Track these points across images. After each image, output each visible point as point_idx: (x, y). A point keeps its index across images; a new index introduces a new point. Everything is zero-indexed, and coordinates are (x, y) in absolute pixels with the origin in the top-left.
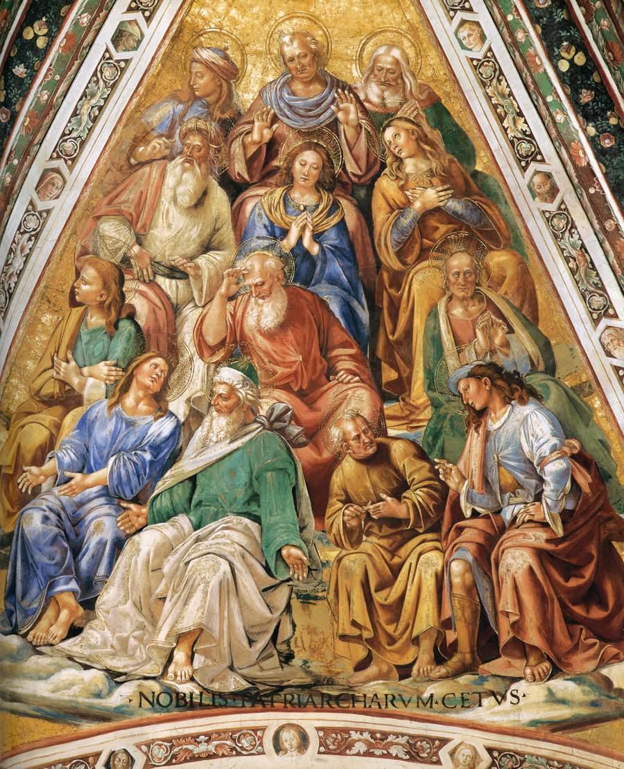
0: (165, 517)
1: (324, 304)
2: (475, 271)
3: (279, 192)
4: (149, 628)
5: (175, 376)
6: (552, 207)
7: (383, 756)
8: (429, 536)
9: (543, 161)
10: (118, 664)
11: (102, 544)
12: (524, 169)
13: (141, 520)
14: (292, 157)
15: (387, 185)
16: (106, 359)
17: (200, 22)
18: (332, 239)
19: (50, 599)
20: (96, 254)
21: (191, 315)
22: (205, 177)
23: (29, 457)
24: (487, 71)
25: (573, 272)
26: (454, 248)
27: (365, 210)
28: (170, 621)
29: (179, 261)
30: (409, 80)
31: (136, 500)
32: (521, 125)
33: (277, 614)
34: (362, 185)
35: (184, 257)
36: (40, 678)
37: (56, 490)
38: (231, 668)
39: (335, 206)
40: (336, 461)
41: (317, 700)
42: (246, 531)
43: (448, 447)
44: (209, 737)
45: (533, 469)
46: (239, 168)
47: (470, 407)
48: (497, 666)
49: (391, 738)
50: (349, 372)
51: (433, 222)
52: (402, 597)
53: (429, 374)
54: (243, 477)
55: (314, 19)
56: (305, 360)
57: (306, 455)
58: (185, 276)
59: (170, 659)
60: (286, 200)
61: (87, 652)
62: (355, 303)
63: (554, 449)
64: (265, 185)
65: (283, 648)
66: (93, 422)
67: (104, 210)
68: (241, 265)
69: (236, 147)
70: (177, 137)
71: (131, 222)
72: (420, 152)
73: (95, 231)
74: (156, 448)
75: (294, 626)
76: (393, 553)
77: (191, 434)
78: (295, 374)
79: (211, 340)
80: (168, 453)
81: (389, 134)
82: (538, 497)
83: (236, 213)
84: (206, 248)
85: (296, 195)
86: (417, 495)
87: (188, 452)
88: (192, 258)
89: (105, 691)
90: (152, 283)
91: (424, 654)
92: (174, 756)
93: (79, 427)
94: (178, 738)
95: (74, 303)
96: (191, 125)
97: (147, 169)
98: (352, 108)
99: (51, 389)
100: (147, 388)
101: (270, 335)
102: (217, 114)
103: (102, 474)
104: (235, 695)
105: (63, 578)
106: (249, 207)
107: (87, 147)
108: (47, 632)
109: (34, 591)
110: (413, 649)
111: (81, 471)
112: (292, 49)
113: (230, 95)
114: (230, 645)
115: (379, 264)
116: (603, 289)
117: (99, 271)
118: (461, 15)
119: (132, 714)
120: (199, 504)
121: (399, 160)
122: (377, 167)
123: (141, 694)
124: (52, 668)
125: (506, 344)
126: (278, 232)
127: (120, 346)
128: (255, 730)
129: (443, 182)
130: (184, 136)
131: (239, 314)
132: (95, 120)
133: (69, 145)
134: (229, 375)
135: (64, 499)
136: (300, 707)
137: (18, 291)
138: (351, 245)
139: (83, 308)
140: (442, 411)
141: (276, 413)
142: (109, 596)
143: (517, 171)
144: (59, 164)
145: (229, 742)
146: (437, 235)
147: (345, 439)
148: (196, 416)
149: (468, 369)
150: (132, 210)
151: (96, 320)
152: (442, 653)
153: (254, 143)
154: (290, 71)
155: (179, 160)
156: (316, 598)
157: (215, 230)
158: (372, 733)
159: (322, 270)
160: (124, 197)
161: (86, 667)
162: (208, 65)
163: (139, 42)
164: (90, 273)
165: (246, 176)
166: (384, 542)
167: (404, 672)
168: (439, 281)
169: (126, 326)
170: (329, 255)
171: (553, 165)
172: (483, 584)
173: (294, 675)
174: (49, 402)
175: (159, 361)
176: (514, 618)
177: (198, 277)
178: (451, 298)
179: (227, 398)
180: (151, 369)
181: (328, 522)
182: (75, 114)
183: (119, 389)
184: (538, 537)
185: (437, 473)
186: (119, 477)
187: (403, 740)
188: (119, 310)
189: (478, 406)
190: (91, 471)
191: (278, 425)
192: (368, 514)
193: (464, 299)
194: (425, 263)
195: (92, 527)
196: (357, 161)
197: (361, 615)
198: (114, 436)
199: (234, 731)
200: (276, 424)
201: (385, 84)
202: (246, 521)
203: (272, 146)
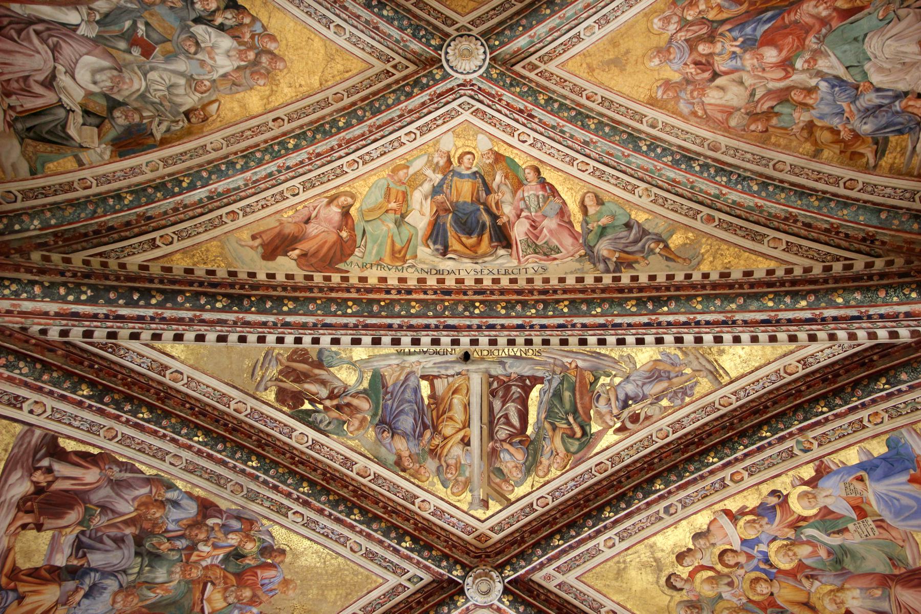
0: (865, 74)
1: (765, 32)
3: (716, 58)
11: (878, 97)
14: (701, 55)
15: (711, 15)
18: (736, 33)
19: (904, 111)
21: (772, 85)
23: (836, 137)
27: (723, 22)
29: (748, 93)
30: (667, 13)
31: (857, 89)
39: (721, 34)
40: (836, 9)
42: (871, 39)
46: (707, 75)
54: (847, 47)
55: (644, 56)
57: (834, 24)
58: (754, 90)
60: (719, 54)
62: (765, 19)
68: (749, 68)
69: (697, 78)
71: (730, 114)
74: (833, 86)
77: (826, 73)
79: (782, 74)
80: (837, 82)
81: (689, 18)
84: (741, 83)
85: (717, 51)
87: (835, 73)
88: (746, 88)
95: (767, 131)
98: (679, 34)
99: (805, 134)
100: (805, 97)
101: (780, 51)
103: (845, 105)
106: (723, 69)
109: (900, 120)
112: (656, 61)
113: (676, 83)
115: (746, 12)
121: (700, 13)
127: (785, 109)
132: (687, 133)
134: (799, 64)
142: (902, 87)
144: (706, 144)
147: (827, 8)
148: (819, 74)
151: (774, 121)
155: (704, 99)
157: (734, 80)
162: (664, 93)
164: (753, 127)
169: (776, 110)
174: (811, 133)
175: (792, 94)
177: (754, 84)
180: (796, 96)
183: (806, 106)
188: (770, 113)
198: (827, 104)
200: (820, 41)
201: (669, 23)
203: (697, 63)
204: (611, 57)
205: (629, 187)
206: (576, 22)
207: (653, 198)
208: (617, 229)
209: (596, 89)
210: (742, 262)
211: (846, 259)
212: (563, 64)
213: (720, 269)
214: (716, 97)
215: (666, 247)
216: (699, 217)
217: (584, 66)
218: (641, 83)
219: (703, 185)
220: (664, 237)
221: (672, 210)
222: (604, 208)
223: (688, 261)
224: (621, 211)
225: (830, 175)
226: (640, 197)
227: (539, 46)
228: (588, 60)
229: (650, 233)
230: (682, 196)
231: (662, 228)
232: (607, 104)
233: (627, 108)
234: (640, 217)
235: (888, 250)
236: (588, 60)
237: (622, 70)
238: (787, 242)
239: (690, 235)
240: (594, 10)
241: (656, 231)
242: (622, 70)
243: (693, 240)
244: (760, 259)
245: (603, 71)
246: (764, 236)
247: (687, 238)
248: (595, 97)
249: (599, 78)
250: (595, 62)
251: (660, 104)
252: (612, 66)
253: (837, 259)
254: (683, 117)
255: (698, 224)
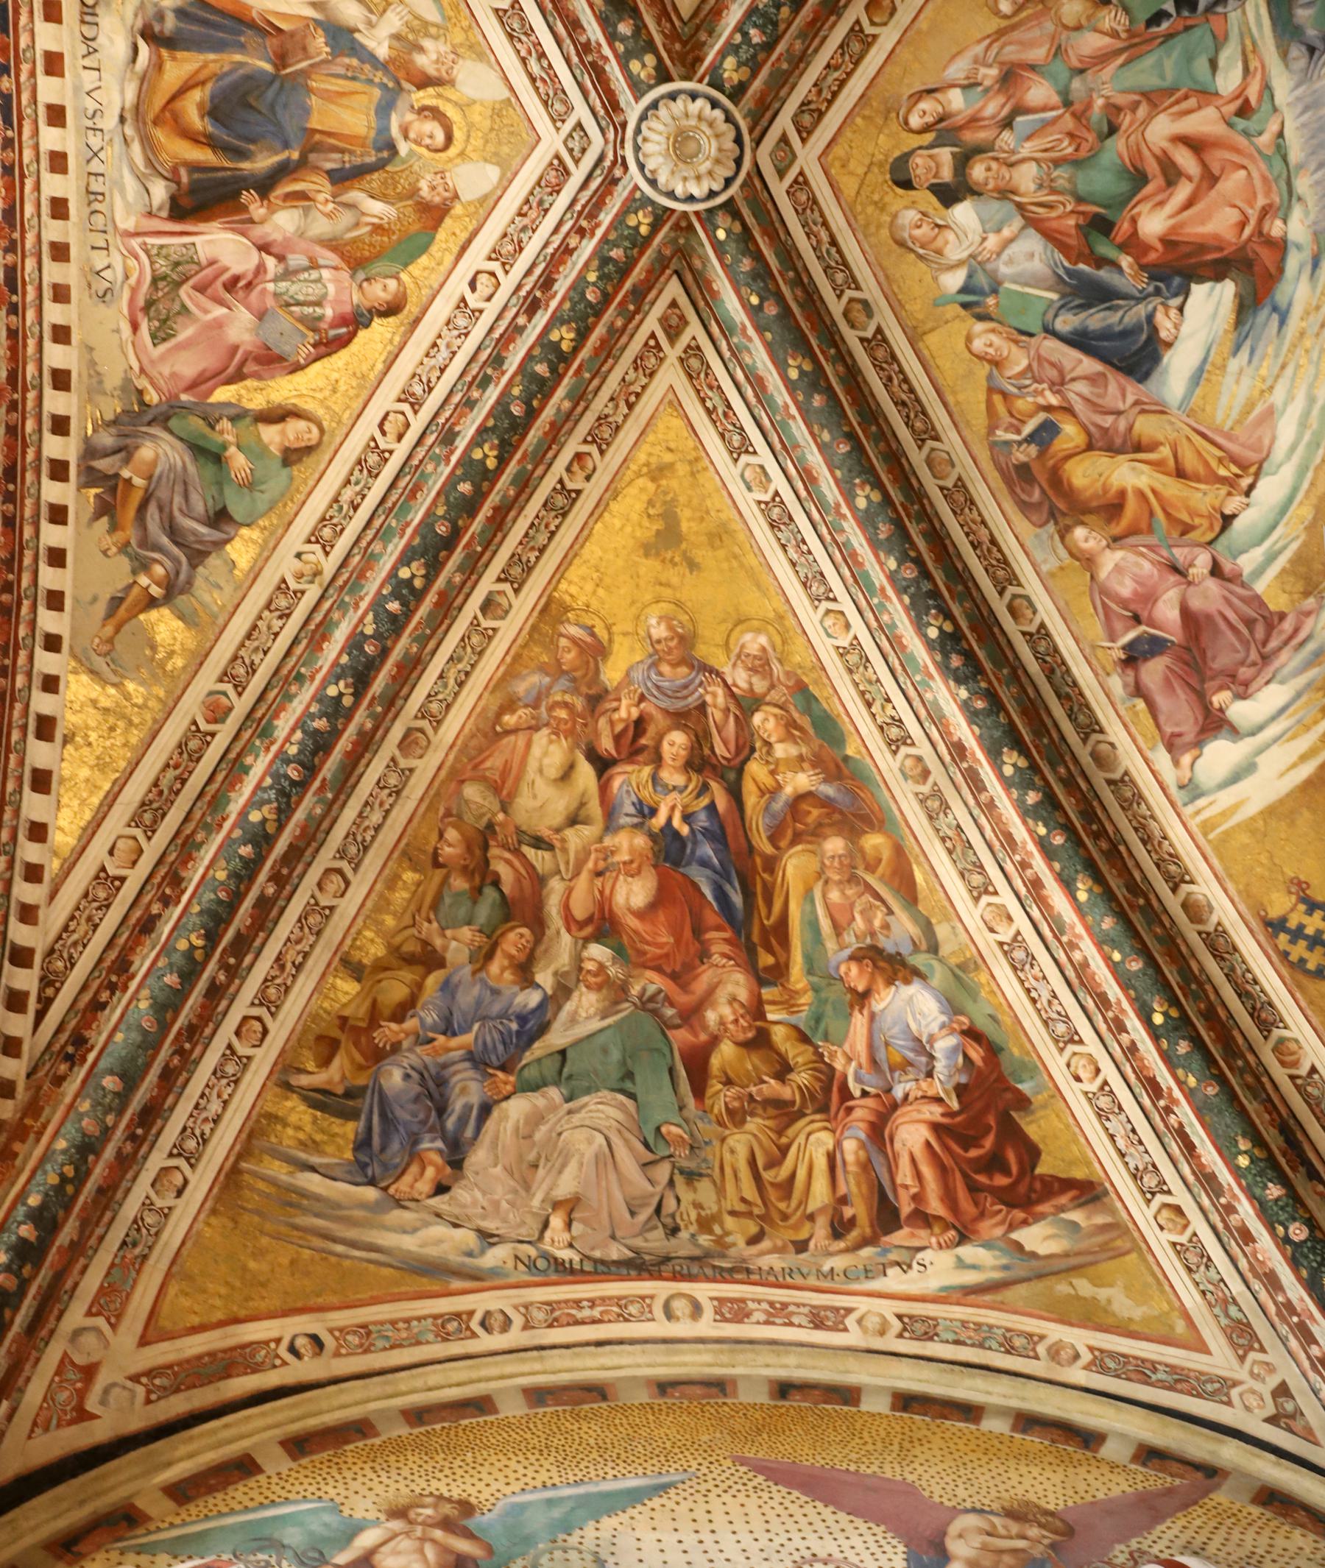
2: (850, 854)
4: (523, 1193)
5: (542, 948)
6: (926, 789)
7: (785, 1324)
8: (818, 1117)
9: (913, 744)
10: (490, 1225)
12: (895, 753)
13: (509, 1088)
16: (469, 923)
17: (567, 598)
20: (460, 817)
22: (571, 750)
24: (853, 658)
25: (950, 852)
26: (827, 831)
28: (545, 1186)
32: (890, 711)
33: (659, 1189)
34: (731, 768)
35: (550, 828)
36: (405, 1232)
37: (418, 1049)
38: (613, 1237)
41: (709, 1272)
43: (831, 1030)
44: (593, 1303)
45: (922, 1047)
47: (852, 991)
48: (901, 1237)
49: (792, 1308)
50: (724, 955)
51: (804, 806)
52: (793, 1176)
53: (809, 959)
56: (678, 941)
59: (546, 1225)
61: (456, 1211)
63: (943, 1026)
64: (632, 762)
65: (668, 1221)
66: (457, 986)
67: (468, 774)
70: (543, 709)
72: (788, 737)
73: (459, 792)
75: (678, 1200)
76: (780, 1133)
78: (667, 956)
82: (930, 1074)
83: (604, 788)
86: (802, 1078)
89: (477, 1251)
90: (517, 852)
91: (821, 1230)
92: (556, 1320)
93: (442, 989)
94: (559, 1302)
96: (558, 698)
97: (512, 738)
102: (584, 690)
104: (618, 1263)
105: (428, 1136)
107: (453, 711)
108: (412, 1187)
110: (808, 1225)
111: (444, 1033)
114: (610, 1216)
116: (982, 867)
117: (462, 834)
118: (825, 605)
119: (507, 1275)
120: (570, 1077)
122: (746, 751)
123: (517, 1257)
124: (418, 1224)
125: (886, 926)
126: (646, 811)
128: (643, 1298)
129: (814, 766)
130: (551, 708)
131: (607, 892)
133: (434, 707)
135: (427, 1059)
136: (690, 1278)
137: (376, 845)
138: (722, 828)
139: (444, 871)
140: (823, 995)
141: (648, 993)
143: (888, 756)
145: (616, 1309)
146: (810, 820)
149: (847, 952)
150: (497, 778)
152: (840, 1228)
153: (621, 720)
154: (656, 652)
156: (701, 1175)
158: (771, 1304)
159: (693, 852)
160: (488, 764)
161: (456, 1226)
163: (507, 612)
165: (614, 752)
166: (768, 1123)
167: (801, 1247)
168: (815, 866)
170: (700, 837)
171: (924, 749)
172: (878, 1162)
173: (682, 1245)
176: (914, 1190)
178: (826, 882)
179: (596, 975)
181: (708, 1102)
182: (441, 677)
184: (934, 1113)
185: (822, 1055)
186: (485, 1043)
187: (806, 1310)
189: (860, 988)
190: (454, 1034)
191: (651, 1006)
192: (751, 1096)
193: (840, 882)
194: (799, 847)
195: (457, 1090)
196: (725, 743)
197: (750, 1191)
199: (620, 1298)
202: (621, 1097)
204: (684, 526)
205: (327, 532)
206: (778, 446)
207: (293, 585)
208: (214, 490)
209: (601, 479)
210: (84, 772)
211: (45, 1004)
212: (677, 405)
213: (69, 720)
214: (546, 761)
215: (152, 603)
216: (228, 688)
217: (668, 457)
218: (608, 589)
219: (302, 699)
220: (181, 600)
221: (254, 627)
222: (276, 464)
223: (105, 648)
224: (262, 506)
225: (287, 990)
226: (299, 555)
227: (723, 345)
228: (682, 469)
229: (193, 566)
230: (288, 653)
231: (206, 598)
232: (560, 501)
233: (542, 550)
234: (241, 550)
235: (39, 1088)
236: (682, 469)
237: (648, 549)
238: (123, 879)
239: (179, 662)
240: (803, 493)
241: (199, 582)
242: (648, 549)
243: (162, 665)
244: (88, 815)
245: (650, 503)
246: (151, 831)
247: (171, 654)
248: (580, 475)
249: (632, 491)
250: (674, 484)
251: (546, 628)
252: (659, 525)
253: (50, 982)
254: (503, 678)
255: (206, 681)
